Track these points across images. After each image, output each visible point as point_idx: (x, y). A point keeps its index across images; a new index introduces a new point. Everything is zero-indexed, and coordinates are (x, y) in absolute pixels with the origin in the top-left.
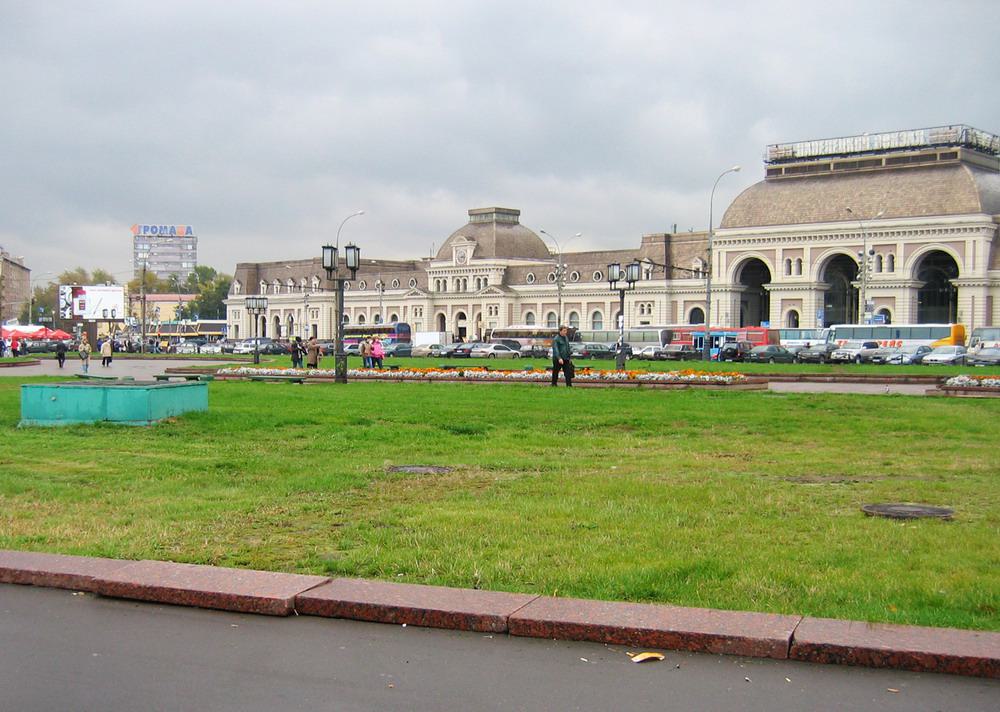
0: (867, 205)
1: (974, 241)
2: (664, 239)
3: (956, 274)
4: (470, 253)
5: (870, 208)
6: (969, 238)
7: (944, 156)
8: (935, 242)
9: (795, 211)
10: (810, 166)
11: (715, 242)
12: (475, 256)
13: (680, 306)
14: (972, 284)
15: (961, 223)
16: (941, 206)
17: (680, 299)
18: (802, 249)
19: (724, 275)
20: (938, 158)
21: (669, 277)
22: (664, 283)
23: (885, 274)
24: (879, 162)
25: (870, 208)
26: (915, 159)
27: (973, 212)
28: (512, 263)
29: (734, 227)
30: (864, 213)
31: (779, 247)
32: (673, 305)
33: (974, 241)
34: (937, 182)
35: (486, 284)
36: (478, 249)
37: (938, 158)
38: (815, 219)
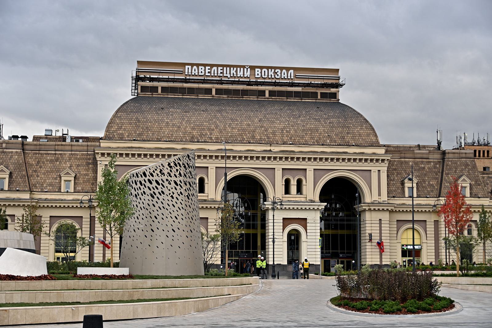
0: (270, 130)
1: (379, 171)
2: (21, 145)
3: (360, 200)
5: (274, 133)
6: (374, 168)
7: (323, 95)
9: (193, 129)
10: (189, 89)
11: (103, 154)
14: (377, 207)
15: (363, 153)
16: (343, 138)
18: (208, 167)
20: (319, 97)
21: (31, 191)
22: (26, 196)
24: (262, 93)
25: (274, 133)
26: (297, 94)
29: (121, 139)
30: (268, 138)
33: (379, 171)
34: (333, 117)
37: (319, 97)
38: (217, 138)
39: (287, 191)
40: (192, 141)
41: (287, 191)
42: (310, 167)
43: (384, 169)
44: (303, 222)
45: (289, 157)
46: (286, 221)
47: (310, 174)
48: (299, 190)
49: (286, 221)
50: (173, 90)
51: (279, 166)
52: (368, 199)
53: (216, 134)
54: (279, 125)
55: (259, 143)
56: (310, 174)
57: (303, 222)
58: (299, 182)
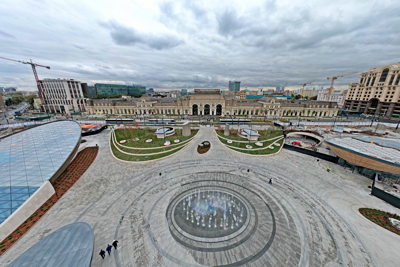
3: (221, 107)
4: (145, 101)
6: (223, 103)
8: (219, 103)
12: (146, 102)
13: (184, 110)
17: (184, 109)
19: (191, 106)
23: (213, 107)
26: (215, 93)
27: (223, 100)
28: (154, 102)
31: (199, 103)
32: (183, 110)
35: (150, 106)
36: (146, 100)
39: (212, 106)
40: (201, 100)
41: (212, 106)
42: (215, 103)
43: (225, 103)
44: (214, 110)
45: (212, 102)
46: (212, 110)
47: (215, 104)
48: (214, 106)
49: (212, 110)
50: (199, 93)
51: (211, 103)
52: (222, 107)
53: (204, 99)
54: (211, 98)
55: (209, 100)
56: (215, 104)
57: (214, 110)
58: (214, 105)
